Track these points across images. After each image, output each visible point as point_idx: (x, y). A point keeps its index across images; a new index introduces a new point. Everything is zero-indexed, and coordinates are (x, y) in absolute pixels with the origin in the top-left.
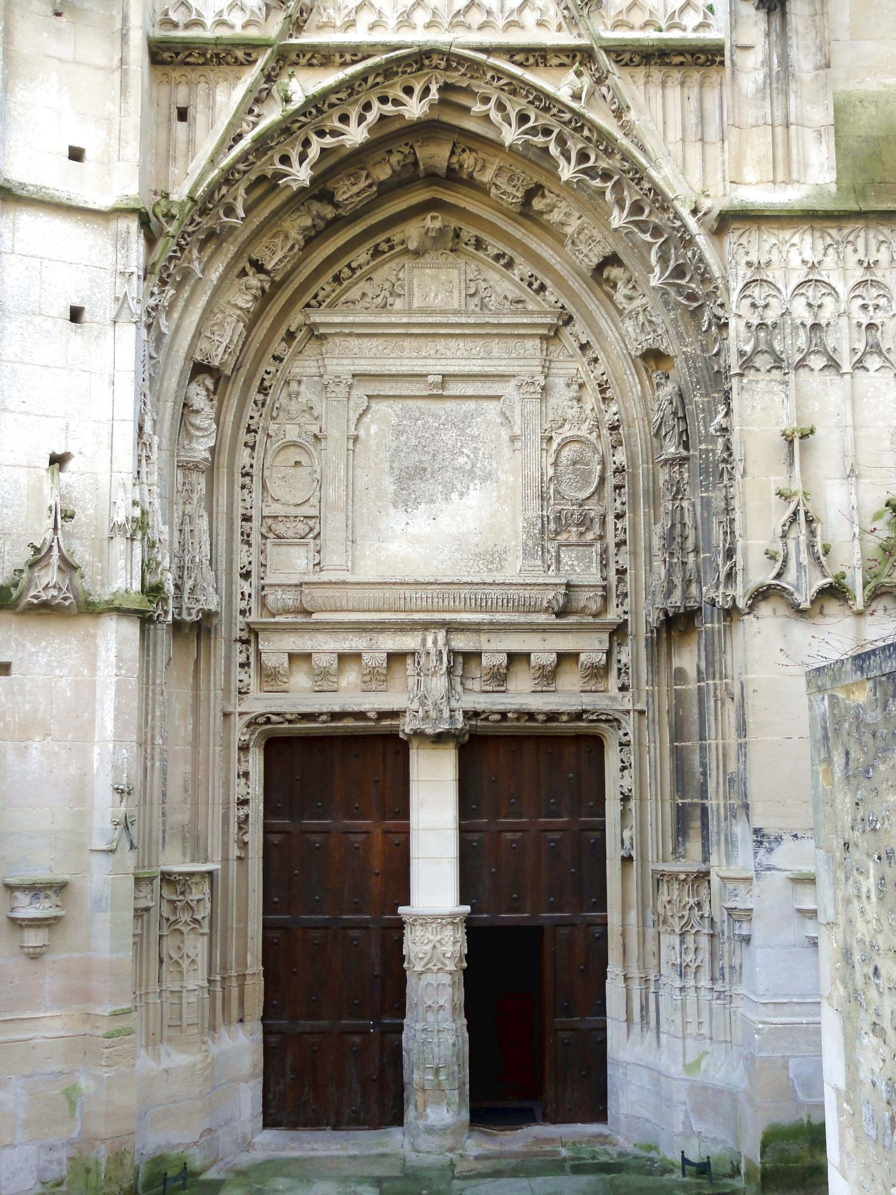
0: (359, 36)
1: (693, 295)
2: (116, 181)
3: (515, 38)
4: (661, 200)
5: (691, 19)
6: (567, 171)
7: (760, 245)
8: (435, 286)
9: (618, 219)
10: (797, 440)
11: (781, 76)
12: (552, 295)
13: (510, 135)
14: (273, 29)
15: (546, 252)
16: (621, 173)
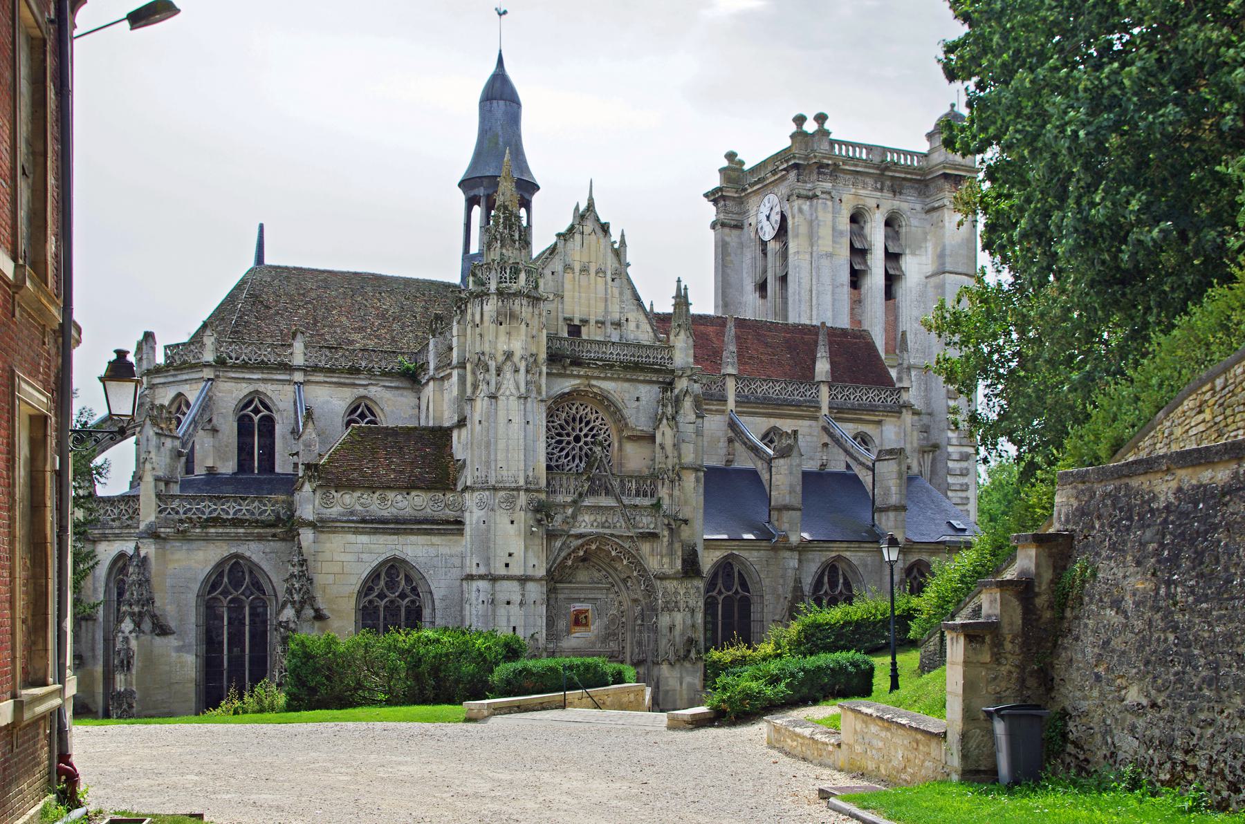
0: (582, 530)
1: (650, 591)
2: (541, 572)
3: (616, 532)
4: (645, 570)
5: (652, 526)
6: (625, 562)
7: (667, 583)
8: (583, 576)
9: (635, 574)
10: (671, 628)
11: (671, 543)
12: (610, 580)
13: (613, 553)
14: (566, 527)
15: (611, 571)
16: (637, 563)
